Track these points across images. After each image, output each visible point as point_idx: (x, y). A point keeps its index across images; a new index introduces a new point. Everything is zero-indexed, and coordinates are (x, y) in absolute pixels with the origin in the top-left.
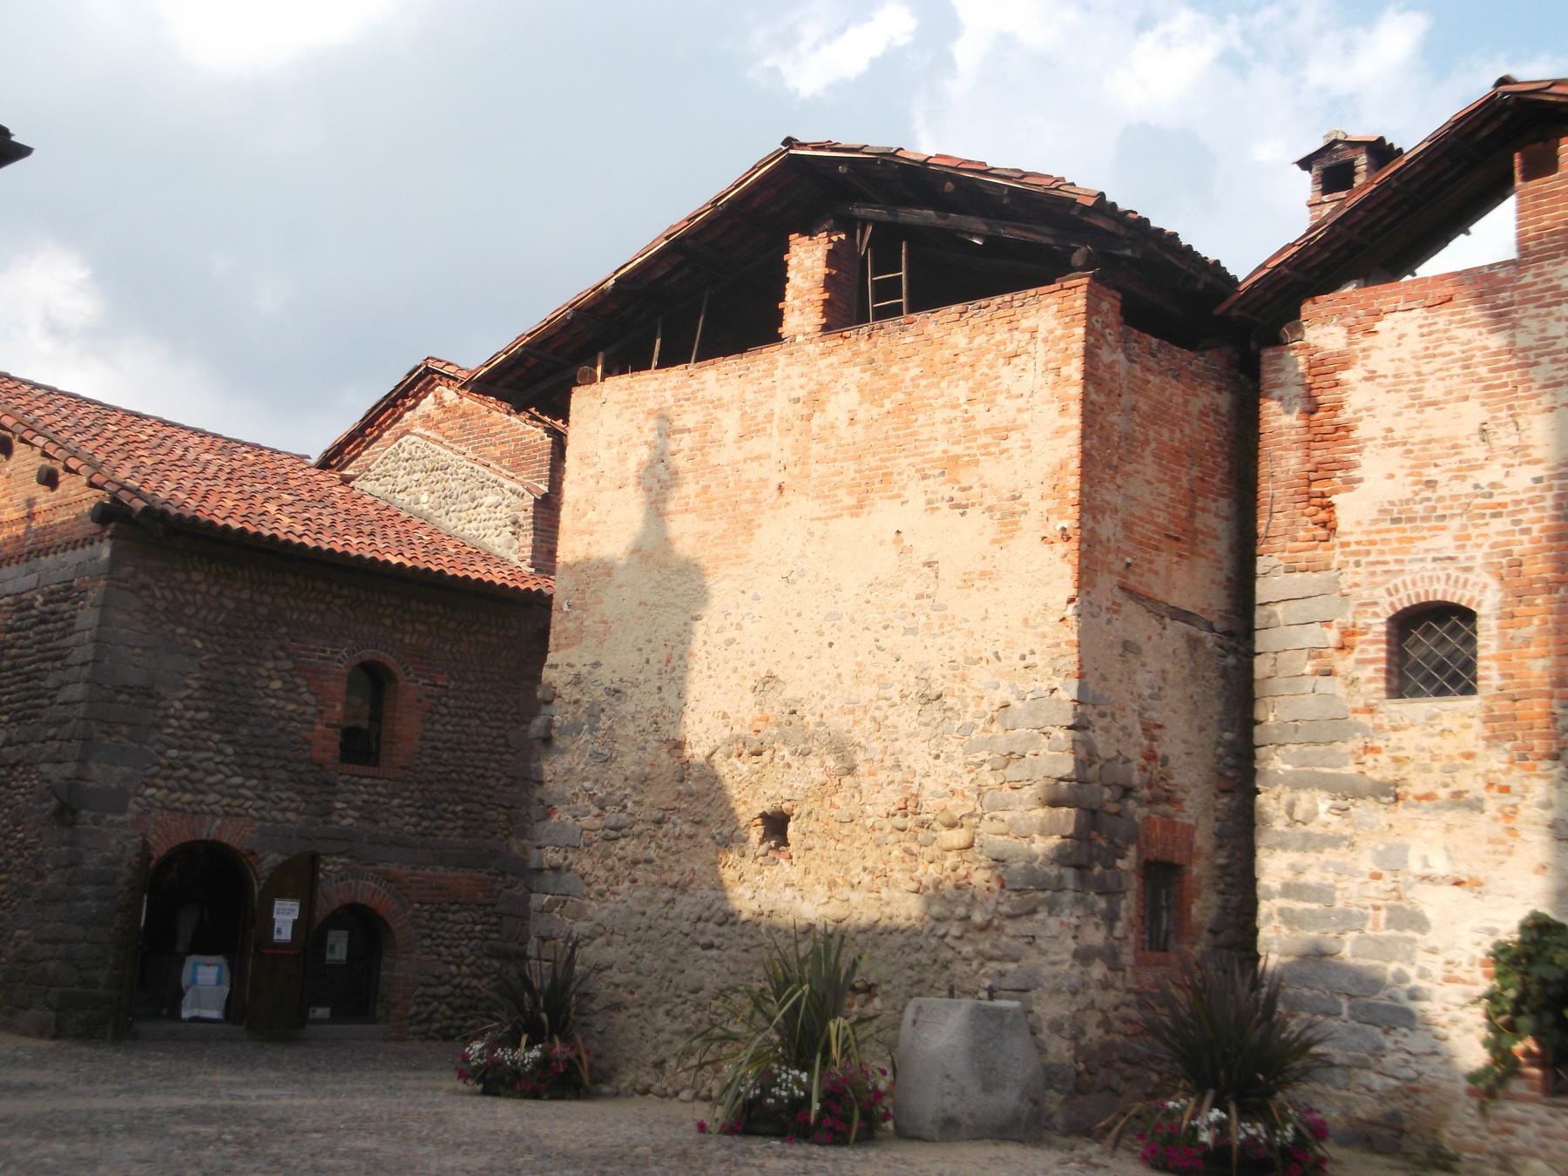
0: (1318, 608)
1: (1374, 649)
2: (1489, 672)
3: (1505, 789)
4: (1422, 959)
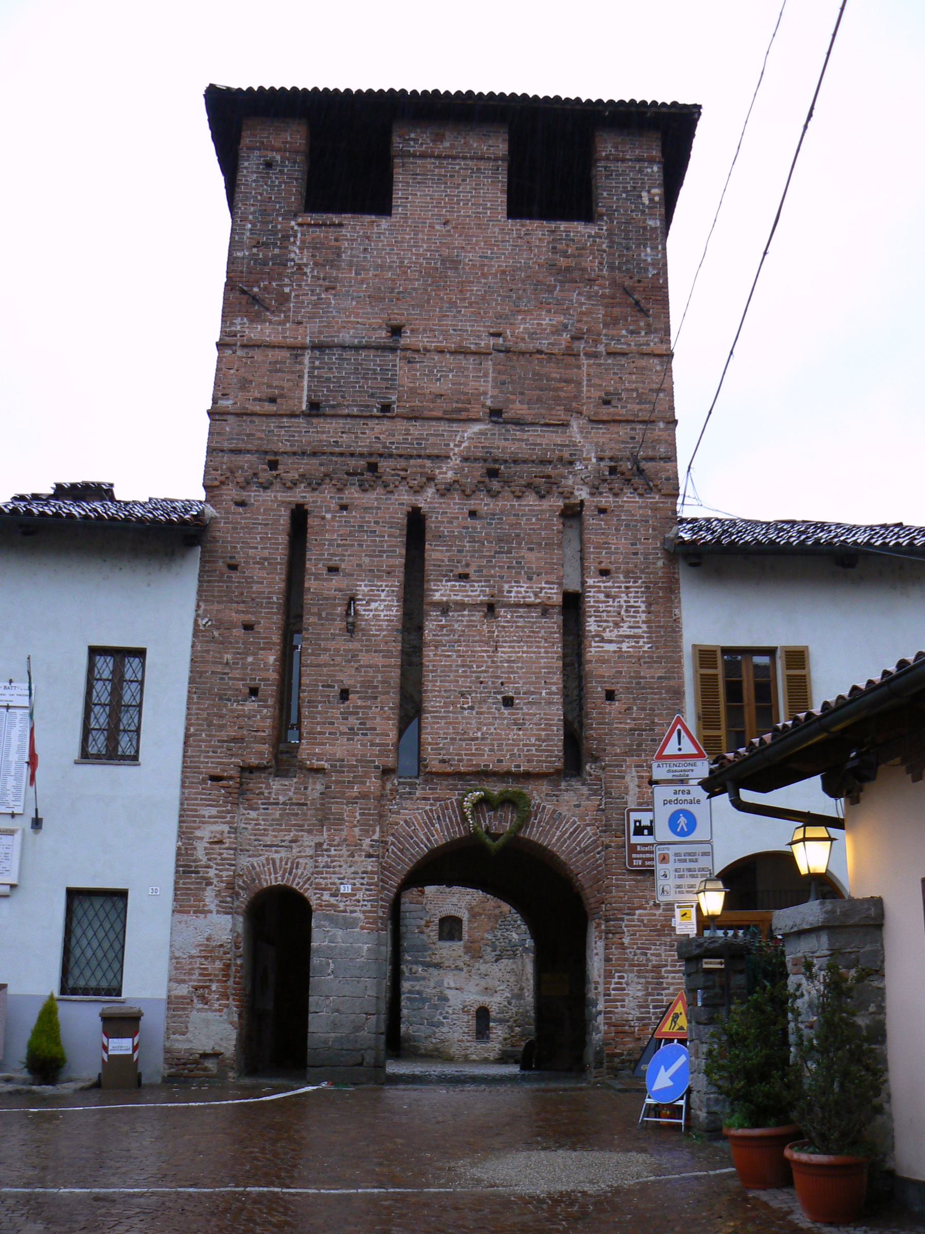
0: (420, 914)
1: (435, 927)
2: (465, 936)
3: (469, 965)
4: (446, 1009)
